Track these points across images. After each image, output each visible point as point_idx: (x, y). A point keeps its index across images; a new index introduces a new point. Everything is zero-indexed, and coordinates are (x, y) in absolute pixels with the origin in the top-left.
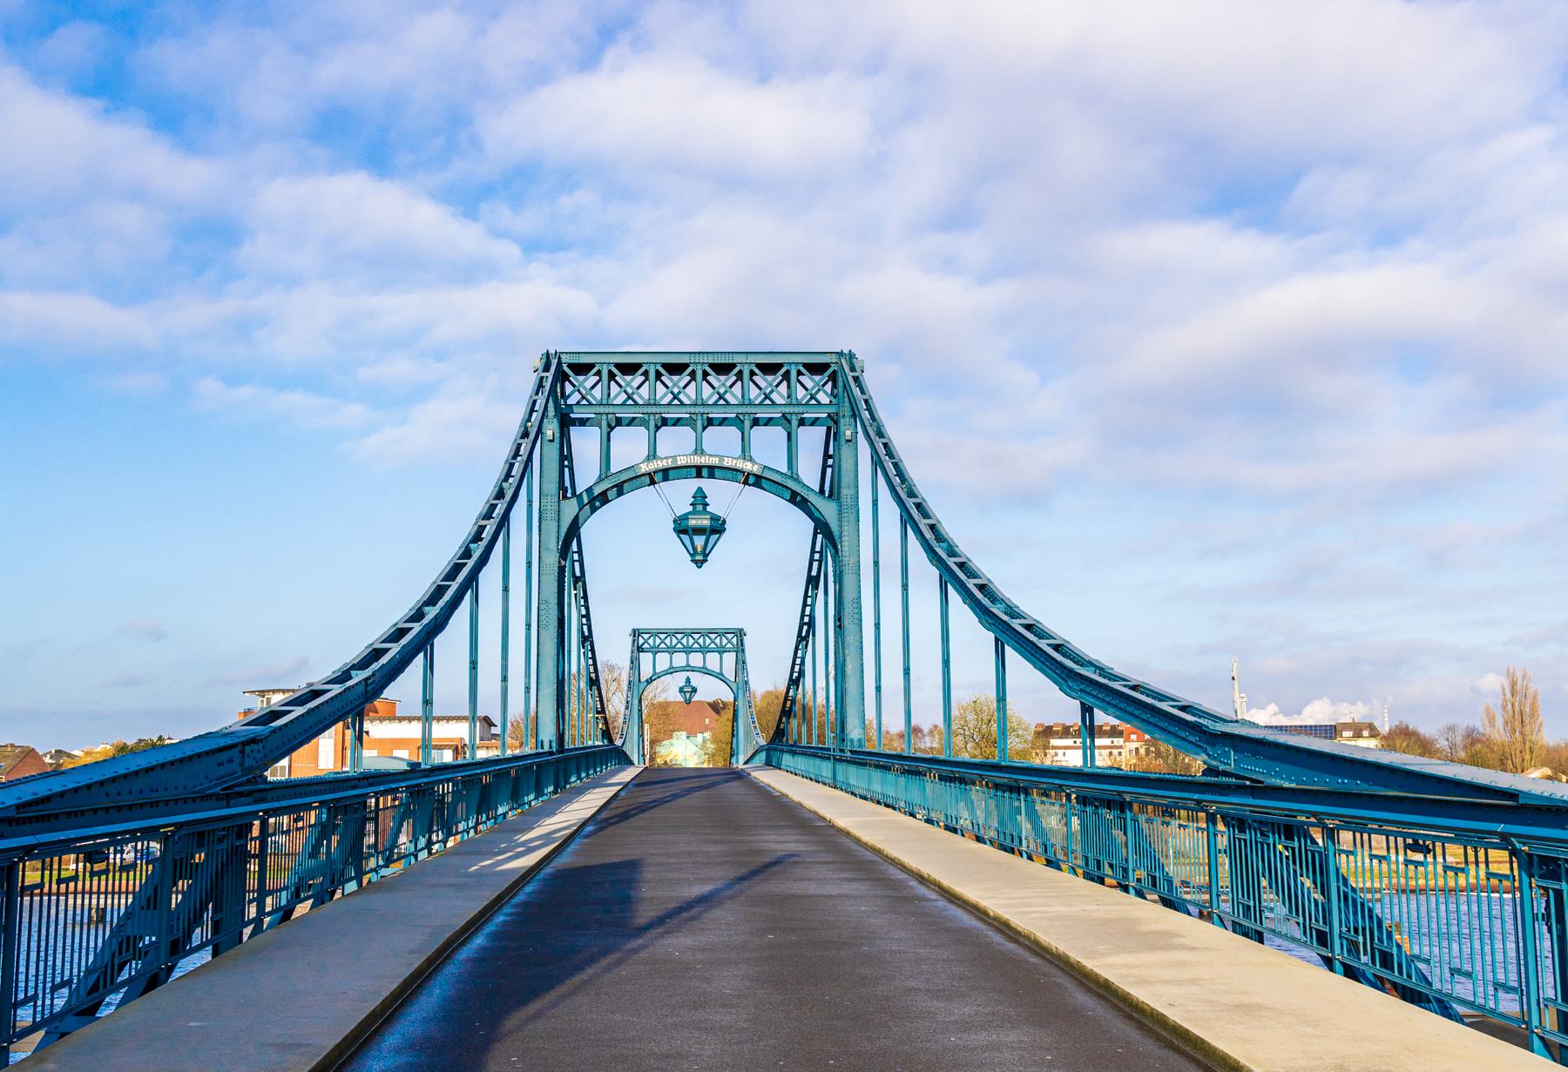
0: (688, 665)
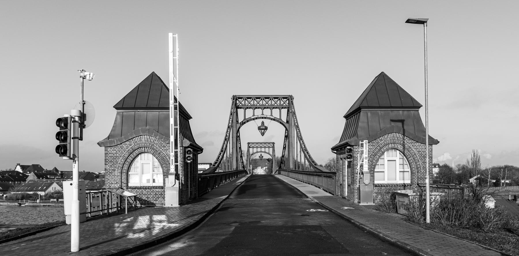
0: (261, 151)
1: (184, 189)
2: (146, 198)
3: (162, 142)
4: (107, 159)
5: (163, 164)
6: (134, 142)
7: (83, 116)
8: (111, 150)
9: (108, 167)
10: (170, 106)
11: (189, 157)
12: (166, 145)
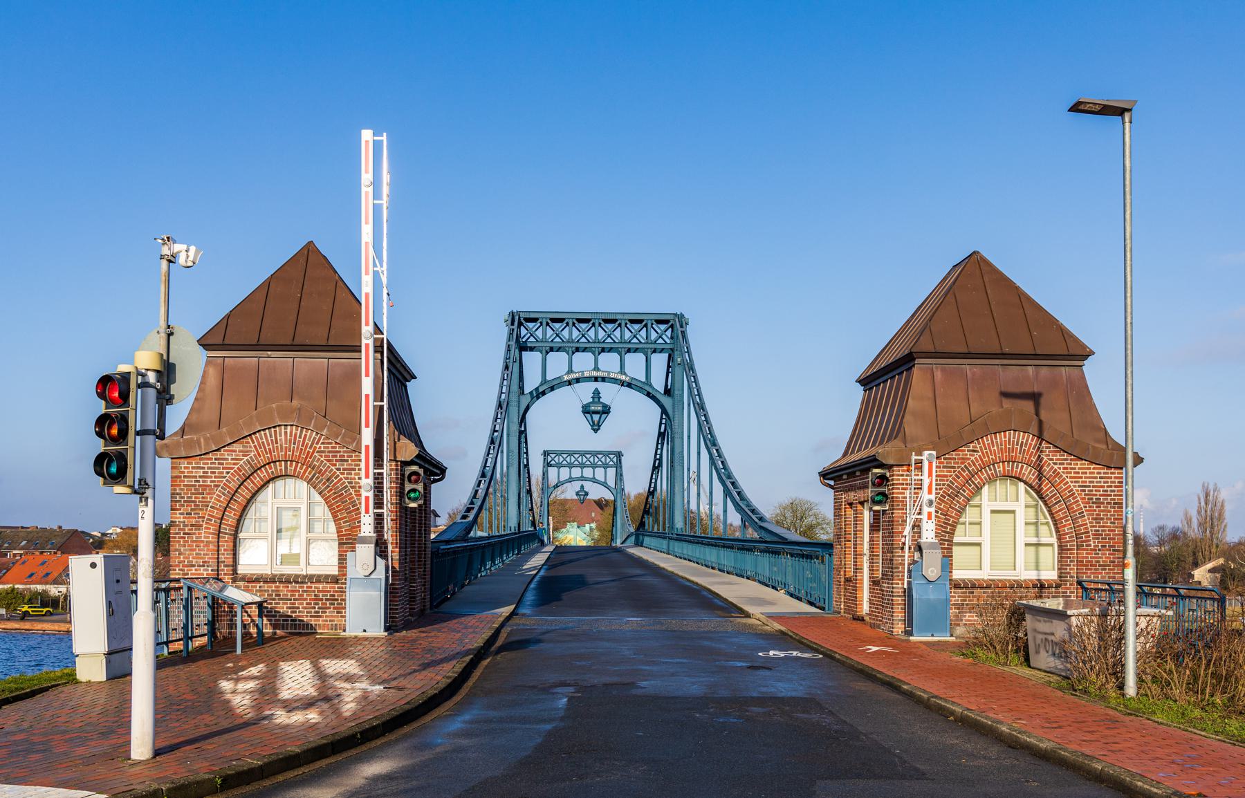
0: (582, 477)
1: (398, 585)
2: (287, 608)
3: (335, 448)
4: (177, 494)
5: (340, 511)
6: (255, 446)
7: (167, 371)
8: (188, 468)
9: (180, 518)
10: (364, 342)
11: (414, 490)
12: (348, 456)
